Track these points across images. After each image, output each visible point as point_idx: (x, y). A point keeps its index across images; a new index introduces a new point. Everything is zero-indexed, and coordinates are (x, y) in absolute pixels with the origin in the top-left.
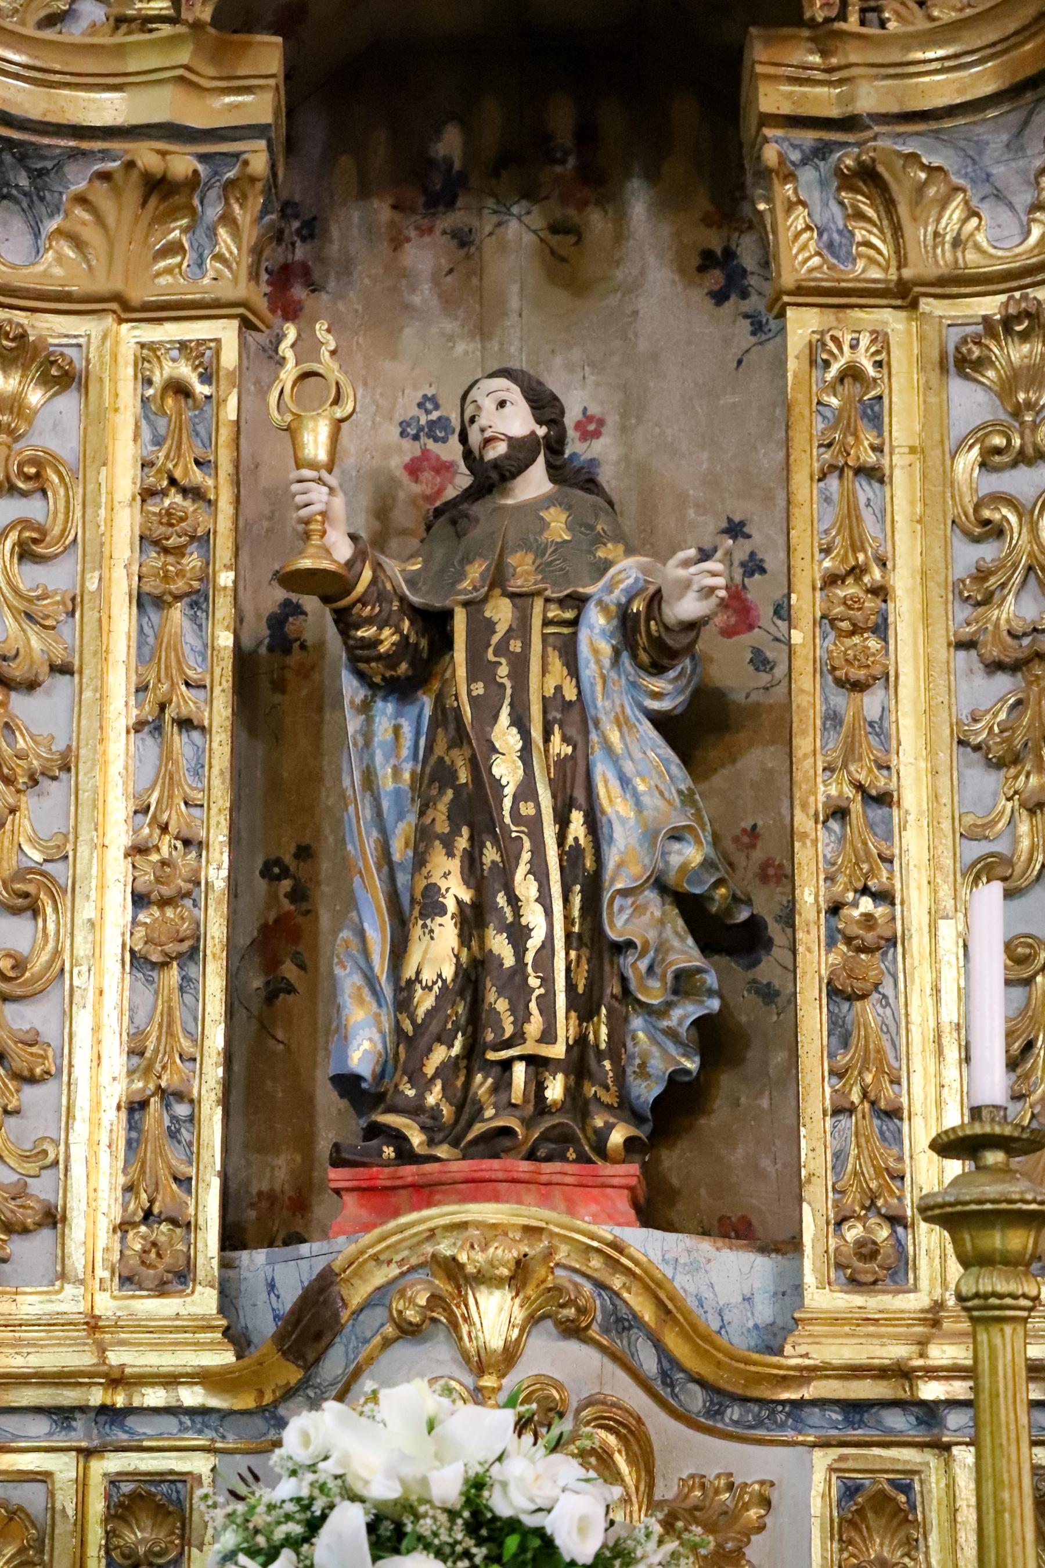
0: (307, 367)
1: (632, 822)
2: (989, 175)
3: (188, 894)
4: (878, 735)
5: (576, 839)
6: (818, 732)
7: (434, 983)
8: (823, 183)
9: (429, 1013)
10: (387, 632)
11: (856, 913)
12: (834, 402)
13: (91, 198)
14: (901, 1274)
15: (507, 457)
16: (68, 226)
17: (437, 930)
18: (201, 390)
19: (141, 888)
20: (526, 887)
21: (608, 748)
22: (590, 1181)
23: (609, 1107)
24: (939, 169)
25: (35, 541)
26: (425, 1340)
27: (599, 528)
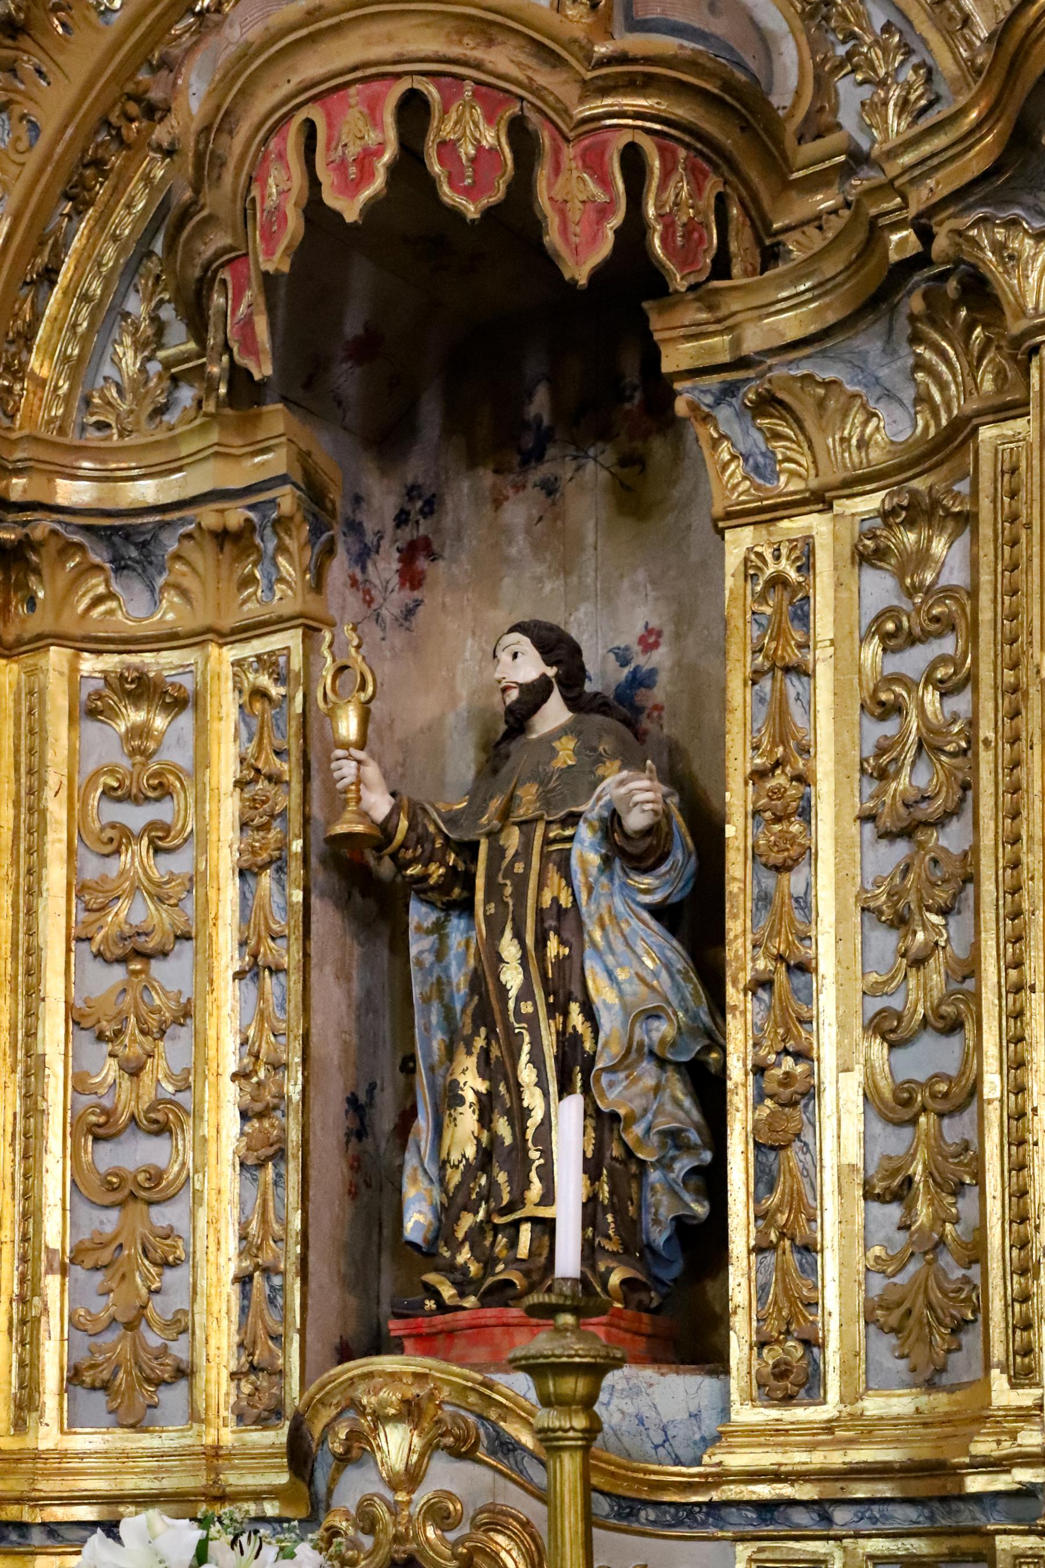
0: (340, 662)
1: (617, 1007)
3: (276, 1108)
4: (802, 909)
5: (574, 1027)
6: (749, 914)
7: (460, 1162)
9: (457, 1187)
12: (769, 611)
13: (184, 554)
14: (815, 1390)
15: (518, 701)
16: (172, 579)
17: (459, 1117)
18: (276, 691)
19: (244, 1108)
20: (527, 1074)
21: (594, 944)
23: (614, 1254)
24: (834, 382)
25: (160, 838)
26: (362, 1465)
27: (601, 749)
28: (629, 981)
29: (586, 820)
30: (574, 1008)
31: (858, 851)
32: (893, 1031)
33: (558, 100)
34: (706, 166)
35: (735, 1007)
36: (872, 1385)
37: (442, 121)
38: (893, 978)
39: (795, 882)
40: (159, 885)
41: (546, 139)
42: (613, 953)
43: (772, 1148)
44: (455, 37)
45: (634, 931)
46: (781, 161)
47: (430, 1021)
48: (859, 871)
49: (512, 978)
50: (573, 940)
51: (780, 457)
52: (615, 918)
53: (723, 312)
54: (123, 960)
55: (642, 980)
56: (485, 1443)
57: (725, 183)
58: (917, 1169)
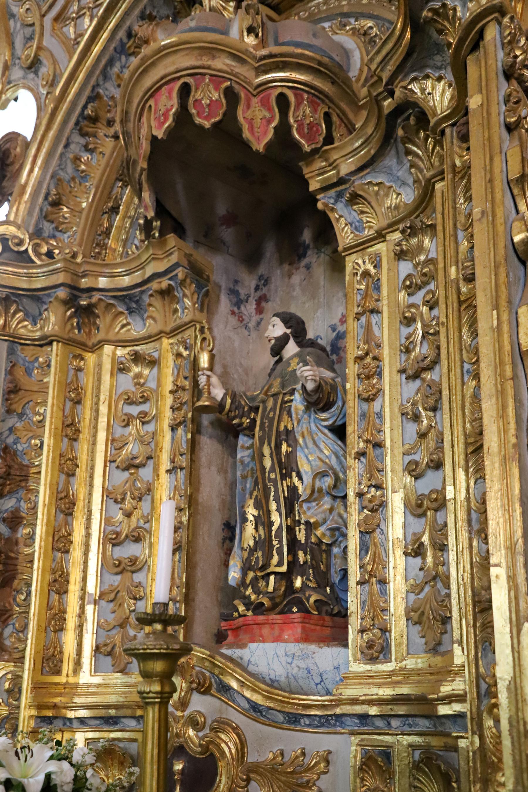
2: (398, 177)
6: (356, 423)
8: (346, 206)
10: (244, 419)
11: (369, 496)
12: (363, 287)
22: (286, 621)
24: (381, 183)
28: (314, 460)
29: (297, 391)
30: (294, 474)
31: (399, 387)
32: (414, 470)
33: (245, 77)
34: (318, 101)
35: (351, 466)
36: (411, 652)
37: (196, 92)
38: (416, 445)
39: (376, 406)
40: (142, 437)
41: (242, 95)
42: (307, 448)
43: (367, 533)
44: (199, 58)
45: (320, 439)
46: (353, 96)
47: (246, 486)
48: (399, 397)
49: (268, 463)
50: (293, 444)
51: (365, 221)
52: (310, 433)
53: (331, 160)
54: (126, 469)
55: (320, 459)
56: (215, 686)
57: (329, 108)
58: (425, 539)
